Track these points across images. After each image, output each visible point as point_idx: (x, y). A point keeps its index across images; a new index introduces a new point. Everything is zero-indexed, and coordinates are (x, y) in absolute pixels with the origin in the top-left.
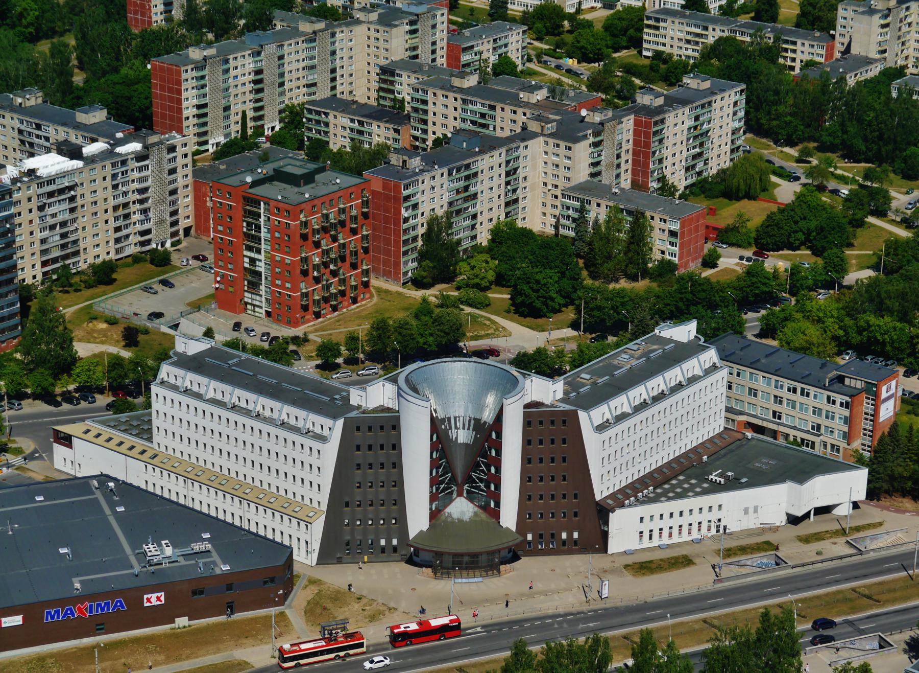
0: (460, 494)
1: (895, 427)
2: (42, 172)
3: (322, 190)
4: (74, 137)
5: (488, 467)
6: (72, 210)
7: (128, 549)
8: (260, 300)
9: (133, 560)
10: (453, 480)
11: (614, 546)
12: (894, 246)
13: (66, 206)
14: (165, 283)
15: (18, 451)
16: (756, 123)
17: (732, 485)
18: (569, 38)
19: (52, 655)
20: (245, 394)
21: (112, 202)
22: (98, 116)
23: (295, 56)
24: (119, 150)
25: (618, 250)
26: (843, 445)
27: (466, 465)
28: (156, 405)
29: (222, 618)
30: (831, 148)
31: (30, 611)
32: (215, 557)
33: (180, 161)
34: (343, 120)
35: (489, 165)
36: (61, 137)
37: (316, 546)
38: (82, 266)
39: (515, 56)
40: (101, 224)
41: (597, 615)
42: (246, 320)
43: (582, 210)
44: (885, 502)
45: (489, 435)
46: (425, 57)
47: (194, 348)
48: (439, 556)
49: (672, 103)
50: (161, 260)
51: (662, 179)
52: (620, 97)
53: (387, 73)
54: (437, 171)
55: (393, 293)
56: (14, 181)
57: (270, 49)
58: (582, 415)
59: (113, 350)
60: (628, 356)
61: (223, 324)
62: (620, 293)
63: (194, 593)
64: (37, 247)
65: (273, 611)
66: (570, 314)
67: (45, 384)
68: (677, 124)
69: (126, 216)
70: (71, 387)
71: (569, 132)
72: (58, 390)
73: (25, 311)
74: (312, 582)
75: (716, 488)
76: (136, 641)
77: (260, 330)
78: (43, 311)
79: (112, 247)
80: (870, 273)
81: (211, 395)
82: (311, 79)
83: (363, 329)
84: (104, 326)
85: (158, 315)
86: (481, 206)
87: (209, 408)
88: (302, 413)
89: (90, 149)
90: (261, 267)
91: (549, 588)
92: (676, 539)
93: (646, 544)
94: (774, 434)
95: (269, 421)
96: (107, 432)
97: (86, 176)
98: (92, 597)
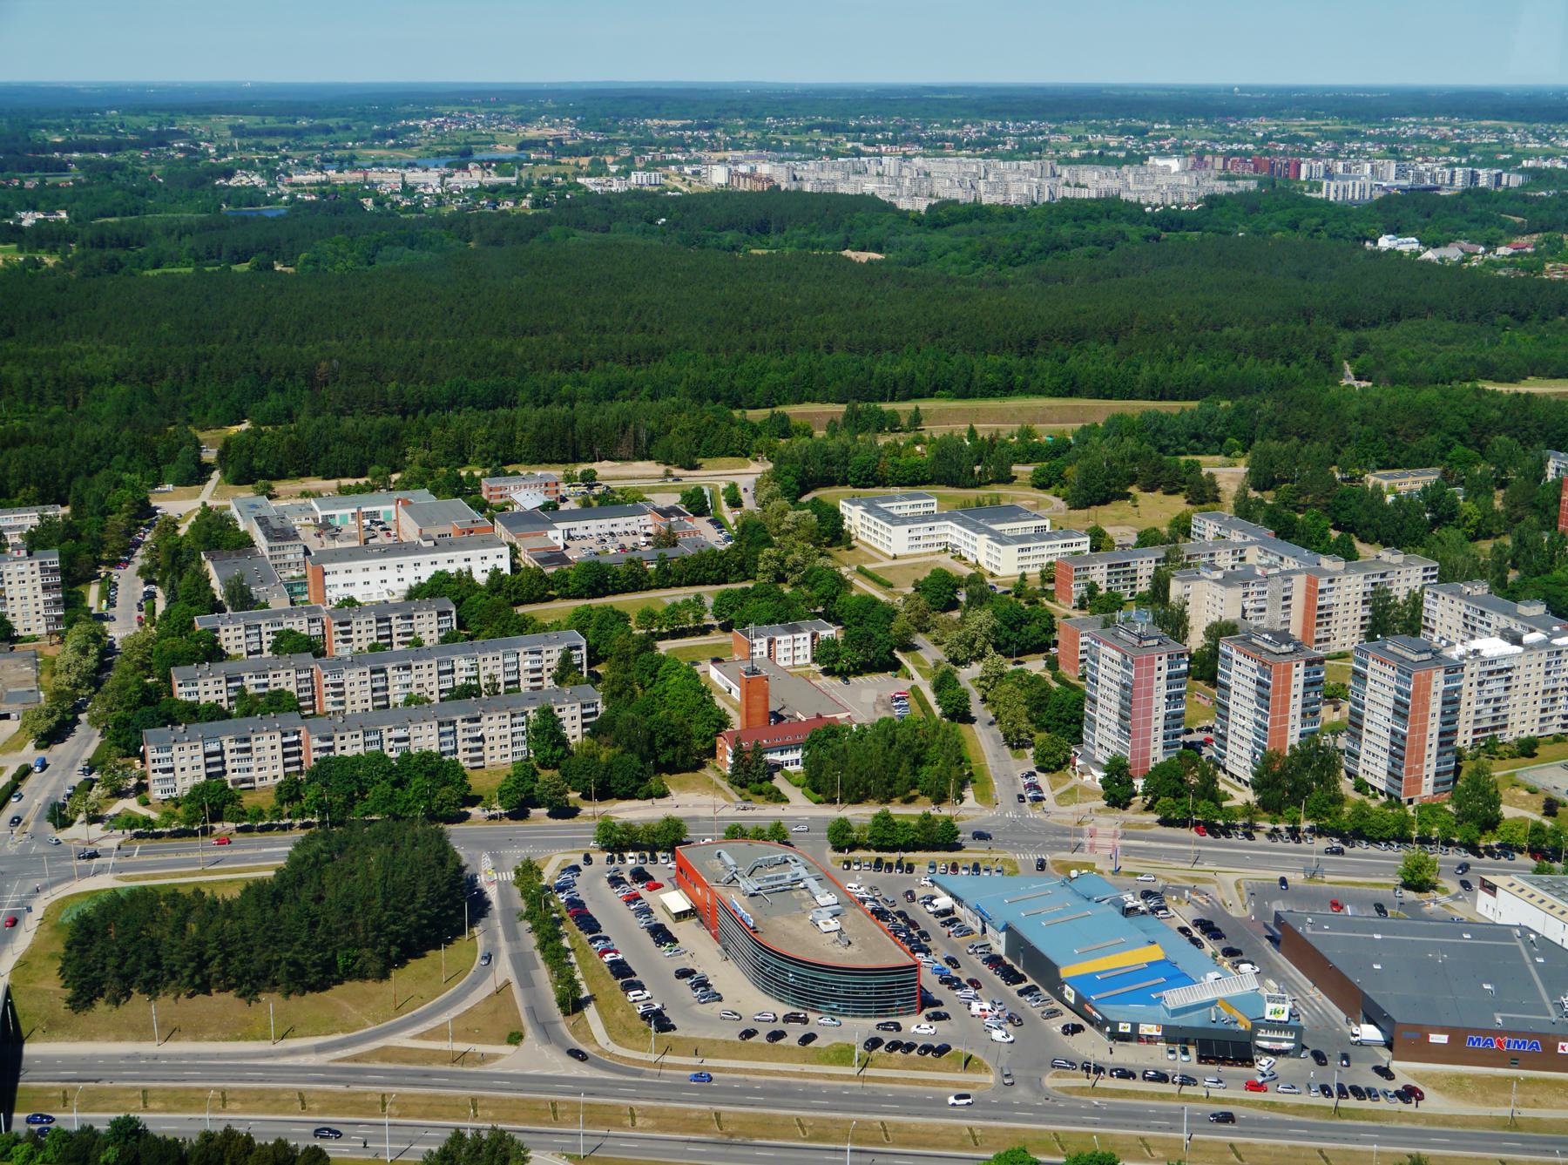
6: (1507, 689)
7: (1546, 999)
9: (1550, 1008)
13: (1503, 684)
15: (1445, 891)
19: (1469, 1077)
21: (1542, 687)
24: (1555, 641)
31: (1456, 1034)
36: (1503, 624)
38: (1508, 738)
40: (1530, 704)
56: (1462, 657)
64: (1472, 716)
67: (1472, 836)
69: (1553, 700)
70: (1494, 843)
72: (1482, 843)
73: (1458, 770)
76: (1546, 1081)
78: (1478, 772)
79: (1536, 725)
84: (1525, 793)
89: (1528, 638)
97: (1524, 661)
98: (1512, 1034)
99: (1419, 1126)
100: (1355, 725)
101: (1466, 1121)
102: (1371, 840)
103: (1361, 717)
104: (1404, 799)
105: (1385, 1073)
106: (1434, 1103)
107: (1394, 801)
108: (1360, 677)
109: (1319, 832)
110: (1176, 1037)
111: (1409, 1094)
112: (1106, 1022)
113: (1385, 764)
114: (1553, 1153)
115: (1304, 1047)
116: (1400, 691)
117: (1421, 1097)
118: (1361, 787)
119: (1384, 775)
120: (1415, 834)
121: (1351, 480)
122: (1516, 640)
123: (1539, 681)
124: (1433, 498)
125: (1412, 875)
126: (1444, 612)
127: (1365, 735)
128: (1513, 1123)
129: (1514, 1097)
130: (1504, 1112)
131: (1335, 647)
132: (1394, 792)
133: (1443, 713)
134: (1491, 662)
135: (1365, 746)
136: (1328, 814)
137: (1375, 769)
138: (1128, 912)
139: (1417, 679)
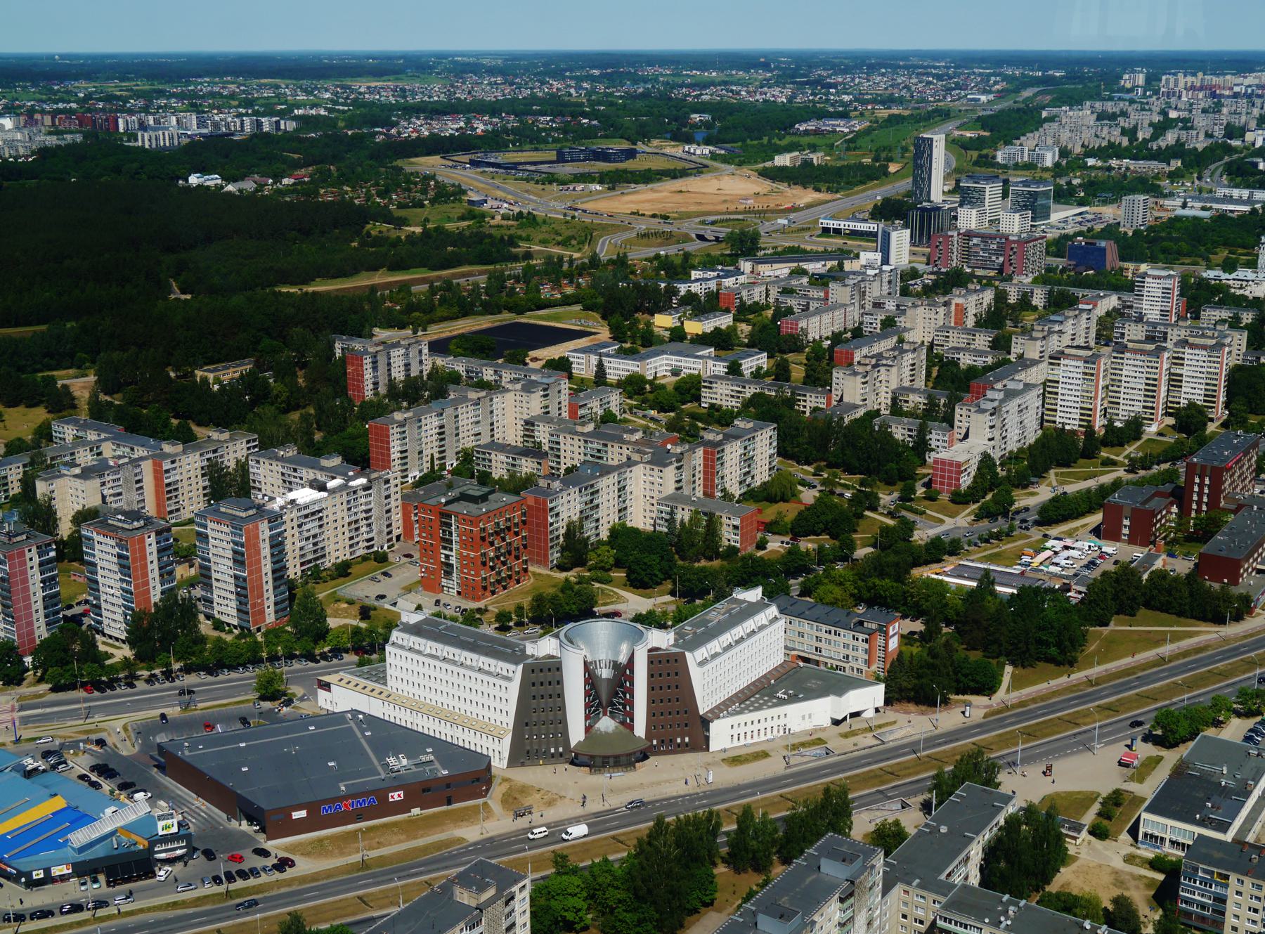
0: (605, 714)
1: (900, 654)
2: (300, 501)
3: (494, 506)
4: (321, 477)
5: (624, 694)
6: (321, 526)
8: (453, 584)
9: (380, 769)
10: (600, 704)
11: (715, 745)
12: (885, 530)
13: (317, 523)
14: (385, 574)
16: (784, 451)
17: (793, 699)
18: (651, 397)
19: (327, 838)
20: (452, 650)
21: (347, 520)
22: (336, 461)
23: (466, 415)
24: (352, 484)
25: (698, 540)
26: (865, 668)
27: (609, 694)
28: (390, 659)
29: (444, 808)
30: (836, 466)
31: (312, 807)
32: (437, 765)
33: (393, 490)
34: (502, 458)
35: (607, 485)
36: (311, 477)
37: (506, 754)
38: (328, 565)
39: (615, 409)
40: (340, 535)
41: (706, 795)
42: (444, 598)
43: (672, 513)
44: (897, 706)
45: (624, 672)
46: (554, 412)
47: (414, 618)
48: (593, 759)
49: (728, 438)
50: (381, 558)
51: (724, 490)
52: (691, 436)
53: (529, 424)
54: (572, 490)
55: (544, 575)
56: (282, 508)
57: (449, 411)
58: (688, 655)
59: (355, 622)
60: (716, 613)
61: (427, 599)
62: (703, 569)
63: (424, 791)
64: (298, 553)
65: (481, 801)
66: (668, 585)
67: (309, 648)
68: (733, 452)
69: (357, 529)
70: (326, 649)
71: (660, 460)
72: (317, 652)
73: (292, 597)
74: (505, 780)
75: (782, 702)
77: (454, 604)
78: (306, 597)
80: (870, 550)
81: (428, 651)
82: (476, 430)
83: (526, 601)
84: (346, 605)
85: (382, 597)
86: (601, 513)
87: (427, 660)
88: (493, 662)
89: (331, 484)
90: (453, 561)
91: (668, 779)
92: (756, 739)
93: (736, 744)
94: (817, 663)
95: (470, 668)
96: (355, 680)
97: (329, 503)
99: (294, 888)
100: (205, 578)
101: (329, 873)
102: (232, 668)
103: (209, 569)
104: (253, 629)
105: (264, 853)
106: (304, 866)
107: (245, 632)
108: (204, 538)
109: (188, 670)
110: (84, 870)
111: (284, 864)
112: (21, 873)
113: (234, 604)
114: (392, 880)
115: (195, 849)
116: (236, 543)
117: (292, 864)
118: (219, 625)
119: (234, 612)
120: (264, 655)
121: (185, 376)
122: (322, 488)
123: (343, 516)
124: (248, 381)
125: (266, 688)
126: (266, 474)
127: (215, 584)
128: (364, 865)
129: (361, 845)
130: (356, 858)
131: (186, 514)
132: (245, 624)
133: (272, 555)
134: (305, 508)
135: (216, 592)
136: (193, 654)
137: (227, 609)
138: (29, 774)
139: (248, 531)
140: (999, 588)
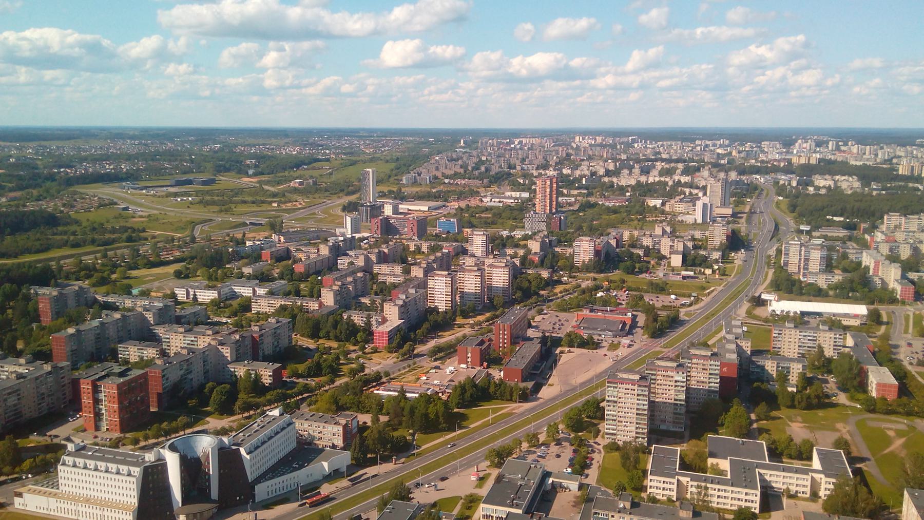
28: (60, 474)
75: (296, 469)
140: (408, 395)
